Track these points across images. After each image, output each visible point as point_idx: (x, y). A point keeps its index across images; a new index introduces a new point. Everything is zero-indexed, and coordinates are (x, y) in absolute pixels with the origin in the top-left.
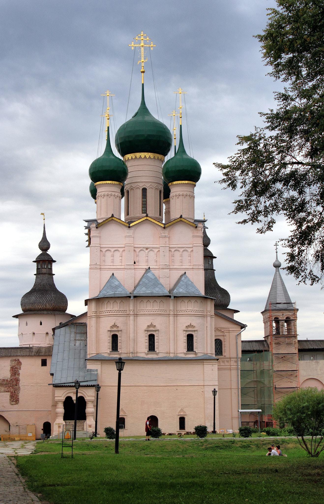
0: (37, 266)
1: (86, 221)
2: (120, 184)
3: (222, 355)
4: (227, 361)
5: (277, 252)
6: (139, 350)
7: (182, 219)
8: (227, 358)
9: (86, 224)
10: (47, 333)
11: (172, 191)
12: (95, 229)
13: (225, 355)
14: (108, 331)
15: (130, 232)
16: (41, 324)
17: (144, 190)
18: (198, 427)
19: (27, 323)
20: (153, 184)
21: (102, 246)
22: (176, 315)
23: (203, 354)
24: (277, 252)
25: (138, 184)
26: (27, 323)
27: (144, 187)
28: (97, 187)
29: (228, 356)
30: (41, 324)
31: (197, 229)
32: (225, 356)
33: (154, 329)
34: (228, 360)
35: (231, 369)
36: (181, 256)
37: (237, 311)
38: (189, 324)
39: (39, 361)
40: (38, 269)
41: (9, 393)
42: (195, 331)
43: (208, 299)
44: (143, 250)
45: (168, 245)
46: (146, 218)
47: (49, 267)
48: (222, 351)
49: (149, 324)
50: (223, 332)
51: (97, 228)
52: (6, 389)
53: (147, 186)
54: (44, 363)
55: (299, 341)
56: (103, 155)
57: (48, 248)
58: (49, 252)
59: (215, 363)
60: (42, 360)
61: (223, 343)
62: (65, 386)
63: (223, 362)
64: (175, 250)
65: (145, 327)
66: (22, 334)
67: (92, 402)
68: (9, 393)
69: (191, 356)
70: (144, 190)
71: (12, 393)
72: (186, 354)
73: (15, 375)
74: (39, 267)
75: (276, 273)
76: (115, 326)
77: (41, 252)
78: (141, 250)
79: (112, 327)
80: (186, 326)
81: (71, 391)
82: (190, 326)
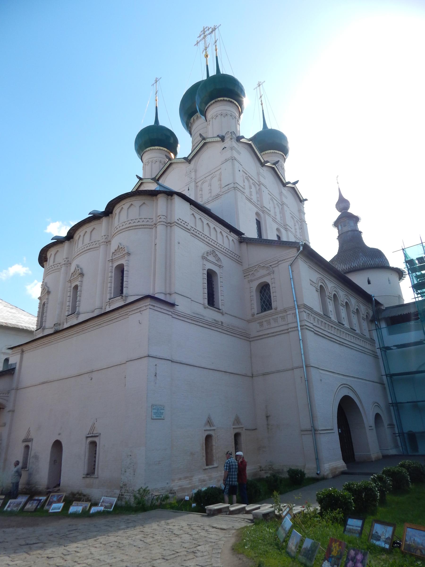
4: (283, 318)
31: (225, 141)
34: (284, 314)
35: (290, 330)
36: (210, 185)
59: (146, 306)
63: (276, 320)
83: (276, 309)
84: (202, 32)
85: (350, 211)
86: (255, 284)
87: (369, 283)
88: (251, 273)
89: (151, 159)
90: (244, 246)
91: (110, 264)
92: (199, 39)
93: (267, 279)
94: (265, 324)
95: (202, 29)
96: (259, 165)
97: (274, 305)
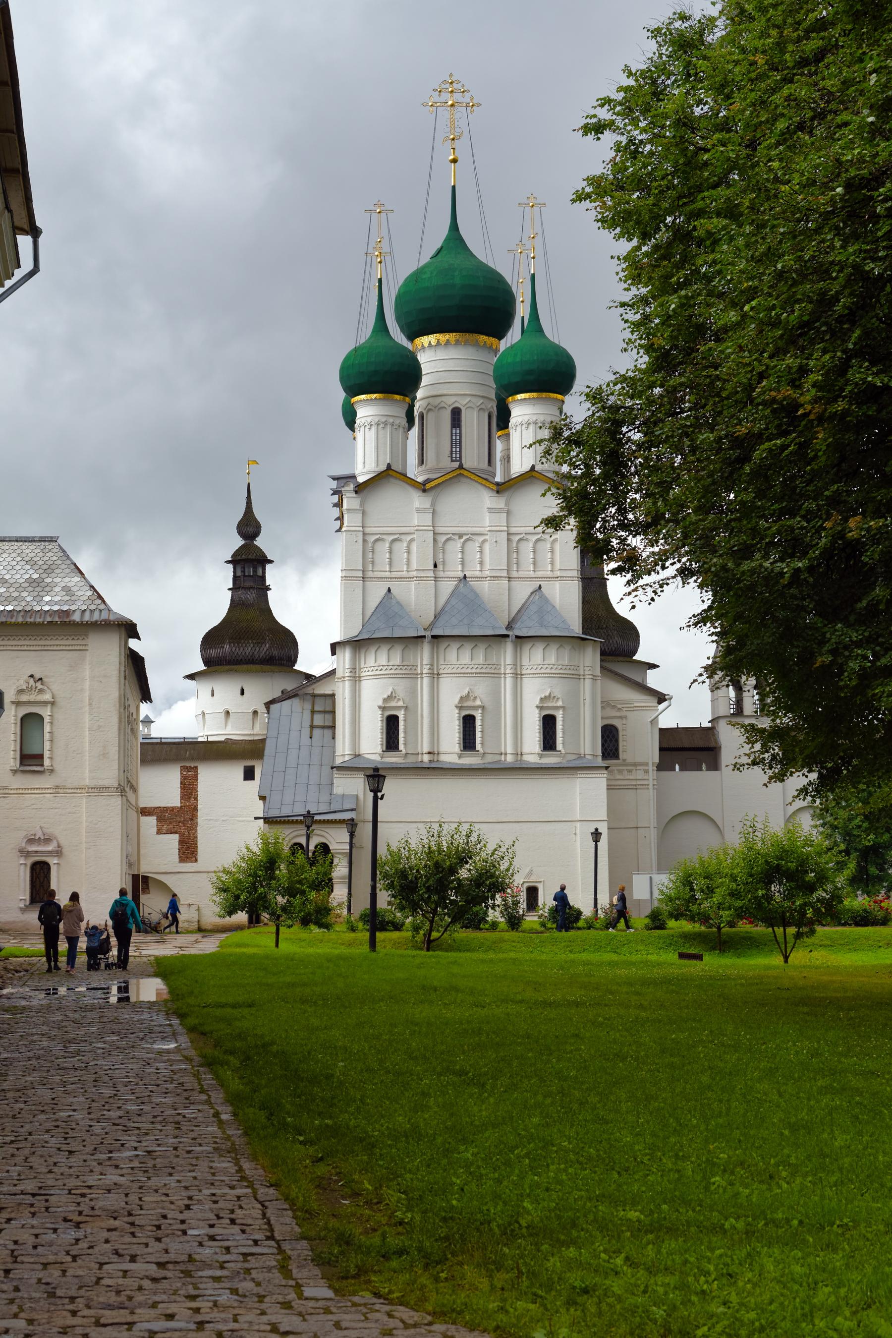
0: (234, 572)
1: (334, 479)
2: (404, 400)
6: (443, 749)
8: (627, 765)
9: (334, 485)
10: (255, 713)
11: (513, 414)
12: (354, 495)
13: (625, 757)
14: (380, 707)
16: (242, 693)
17: (456, 414)
18: (362, 915)
19: (213, 691)
20: (474, 399)
21: (368, 530)
23: (574, 757)
25: (443, 399)
26: (213, 691)
27: (456, 405)
28: (356, 406)
29: (628, 761)
30: (242, 693)
32: (624, 760)
37: (653, 666)
38: (547, 694)
39: (237, 771)
40: (235, 578)
41: (177, 836)
44: (454, 540)
45: (505, 528)
46: (458, 472)
47: (260, 573)
48: (617, 750)
51: (356, 492)
52: (171, 826)
53: (461, 403)
54: (249, 775)
56: (371, 337)
57: (256, 534)
58: (259, 542)
60: (245, 767)
61: (621, 734)
62: (289, 822)
63: (620, 772)
65: (456, 701)
66: (203, 713)
68: (177, 836)
69: (551, 759)
70: (456, 414)
71: (182, 836)
72: (541, 756)
73: (190, 798)
74: (239, 574)
77: (243, 542)
78: (448, 540)
79: (385, 700)
84: (445, 82)
89: (391, 420)
97: (622, 755)
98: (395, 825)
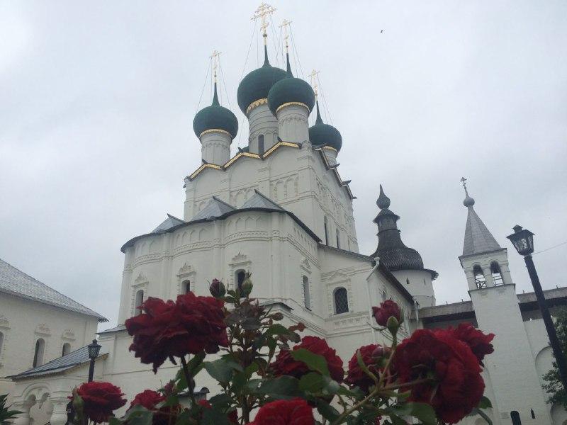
3: (347, 310)
5: (465, 188)
7: (283, 144)
15: (226, 175)
22: (222, 246)
24: (465, 188)
29: (355, 312)
32: (352, 312)
33: (188, 272)
34: (359, 317)
36: (285, 187)
38: (237, 254)
42: (245, 264)
43: (273, 213)
49: (182, 266)
50: (345, 275)
53: (263, 132)
55: (518, 296)
64: (278, 183)
65: (176, 271)
67: (60, 402)
75: (469, 213)
76: (140, 278)
78: (238, 193)
80: (233, 259)
81: (35, 385)
82: (240, 256)
83: (352, 312)
85: (390, 208)
86: (332, 289)
87: (408, 283)
88: (328, 277)
89: (213, 142)
90: (322, 253)
91: (231, 269)
92: (256, 14)
93: (344, 285)
94: (341, 324)
95: (261, 5)
96: (324, 168)
97: (350, 309)
98: (129, 375)
